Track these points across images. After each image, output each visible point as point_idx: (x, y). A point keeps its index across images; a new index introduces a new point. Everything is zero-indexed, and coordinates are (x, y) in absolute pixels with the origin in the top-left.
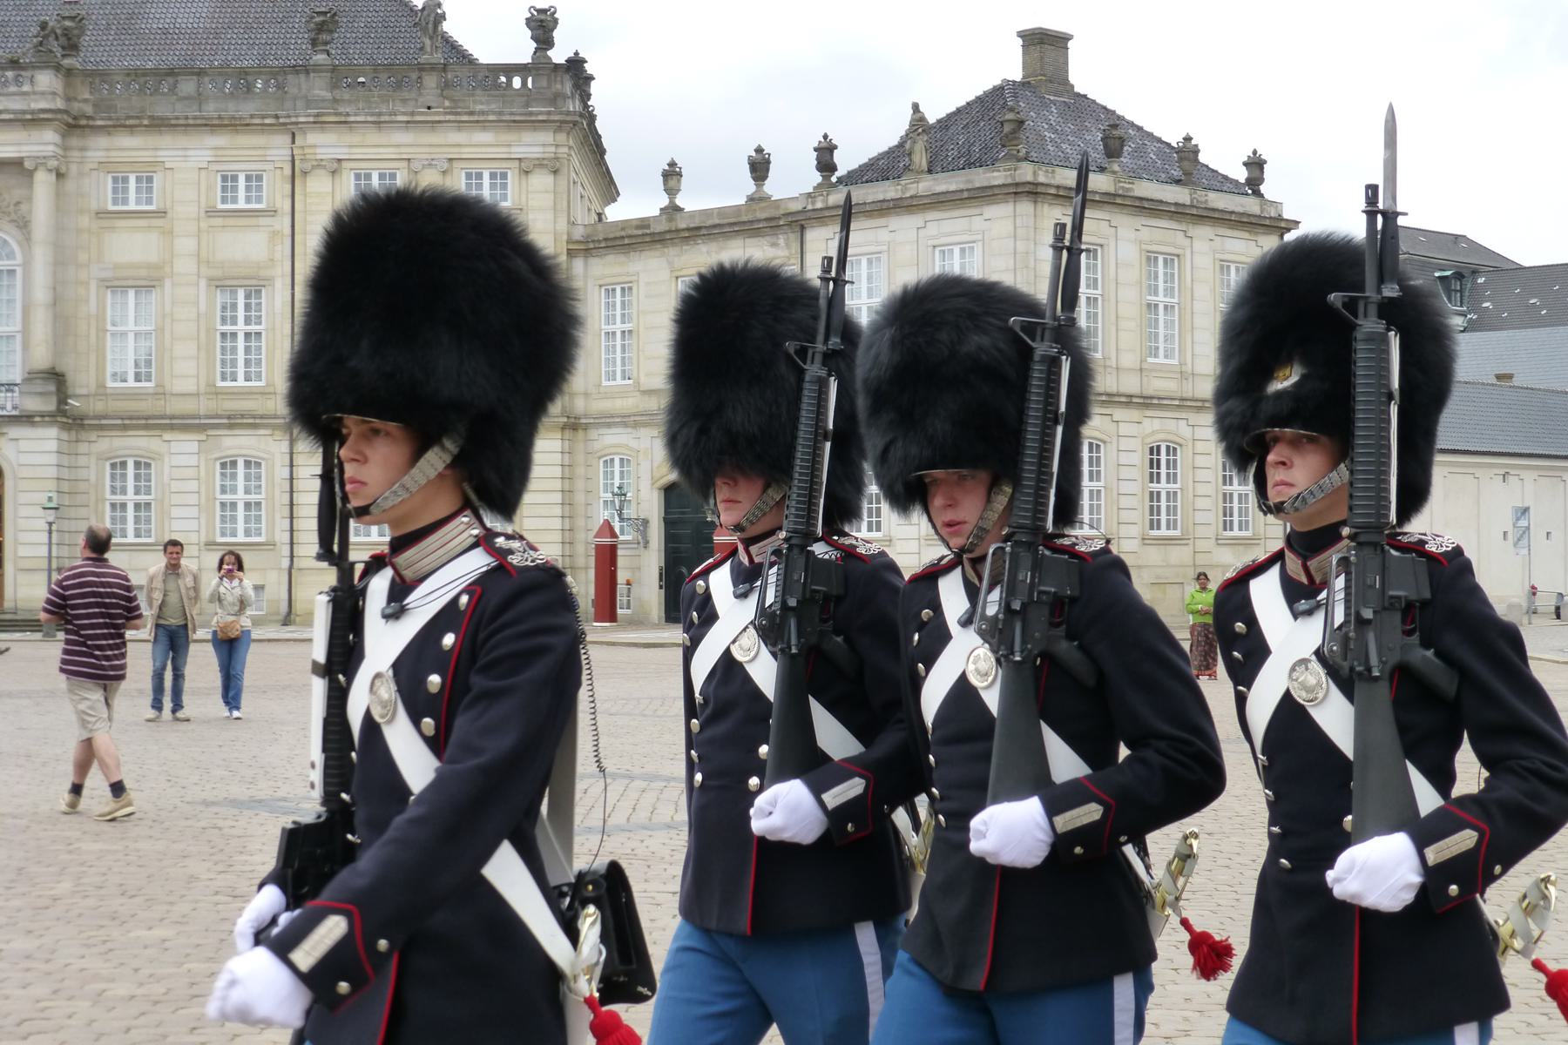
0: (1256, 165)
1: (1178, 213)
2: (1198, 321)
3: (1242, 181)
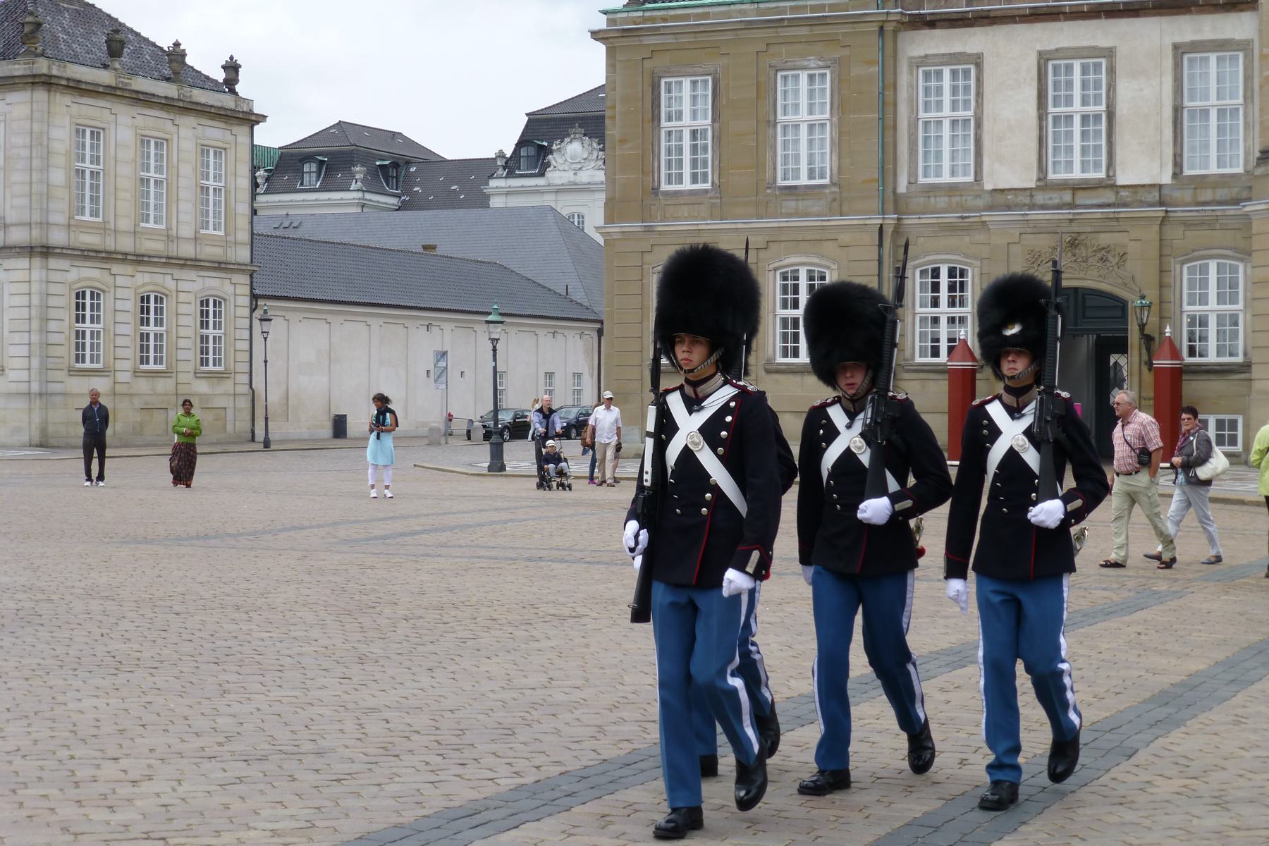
0: (232, 68)
1: (167, 105)
2: (182, 194)
3: (221, 81)
